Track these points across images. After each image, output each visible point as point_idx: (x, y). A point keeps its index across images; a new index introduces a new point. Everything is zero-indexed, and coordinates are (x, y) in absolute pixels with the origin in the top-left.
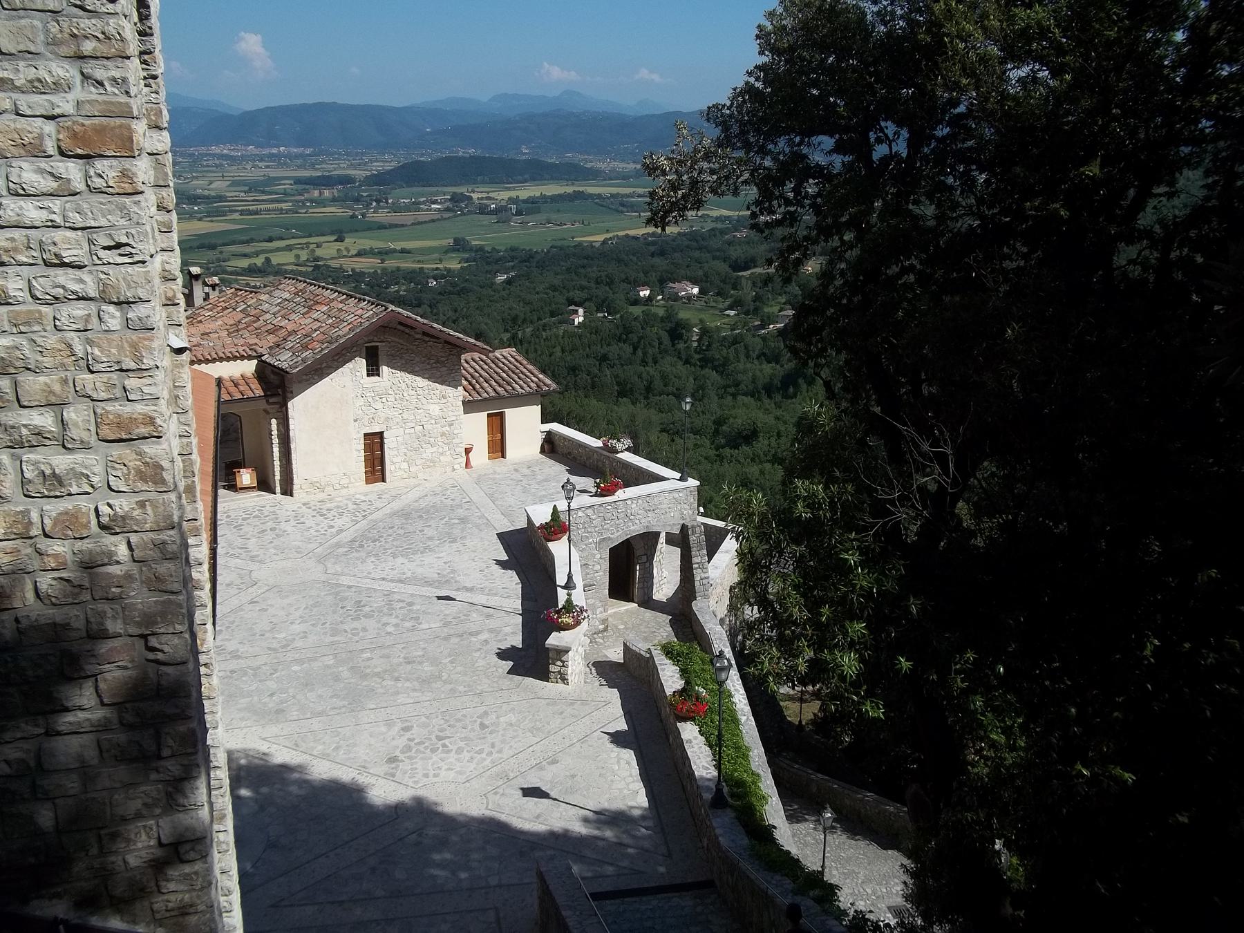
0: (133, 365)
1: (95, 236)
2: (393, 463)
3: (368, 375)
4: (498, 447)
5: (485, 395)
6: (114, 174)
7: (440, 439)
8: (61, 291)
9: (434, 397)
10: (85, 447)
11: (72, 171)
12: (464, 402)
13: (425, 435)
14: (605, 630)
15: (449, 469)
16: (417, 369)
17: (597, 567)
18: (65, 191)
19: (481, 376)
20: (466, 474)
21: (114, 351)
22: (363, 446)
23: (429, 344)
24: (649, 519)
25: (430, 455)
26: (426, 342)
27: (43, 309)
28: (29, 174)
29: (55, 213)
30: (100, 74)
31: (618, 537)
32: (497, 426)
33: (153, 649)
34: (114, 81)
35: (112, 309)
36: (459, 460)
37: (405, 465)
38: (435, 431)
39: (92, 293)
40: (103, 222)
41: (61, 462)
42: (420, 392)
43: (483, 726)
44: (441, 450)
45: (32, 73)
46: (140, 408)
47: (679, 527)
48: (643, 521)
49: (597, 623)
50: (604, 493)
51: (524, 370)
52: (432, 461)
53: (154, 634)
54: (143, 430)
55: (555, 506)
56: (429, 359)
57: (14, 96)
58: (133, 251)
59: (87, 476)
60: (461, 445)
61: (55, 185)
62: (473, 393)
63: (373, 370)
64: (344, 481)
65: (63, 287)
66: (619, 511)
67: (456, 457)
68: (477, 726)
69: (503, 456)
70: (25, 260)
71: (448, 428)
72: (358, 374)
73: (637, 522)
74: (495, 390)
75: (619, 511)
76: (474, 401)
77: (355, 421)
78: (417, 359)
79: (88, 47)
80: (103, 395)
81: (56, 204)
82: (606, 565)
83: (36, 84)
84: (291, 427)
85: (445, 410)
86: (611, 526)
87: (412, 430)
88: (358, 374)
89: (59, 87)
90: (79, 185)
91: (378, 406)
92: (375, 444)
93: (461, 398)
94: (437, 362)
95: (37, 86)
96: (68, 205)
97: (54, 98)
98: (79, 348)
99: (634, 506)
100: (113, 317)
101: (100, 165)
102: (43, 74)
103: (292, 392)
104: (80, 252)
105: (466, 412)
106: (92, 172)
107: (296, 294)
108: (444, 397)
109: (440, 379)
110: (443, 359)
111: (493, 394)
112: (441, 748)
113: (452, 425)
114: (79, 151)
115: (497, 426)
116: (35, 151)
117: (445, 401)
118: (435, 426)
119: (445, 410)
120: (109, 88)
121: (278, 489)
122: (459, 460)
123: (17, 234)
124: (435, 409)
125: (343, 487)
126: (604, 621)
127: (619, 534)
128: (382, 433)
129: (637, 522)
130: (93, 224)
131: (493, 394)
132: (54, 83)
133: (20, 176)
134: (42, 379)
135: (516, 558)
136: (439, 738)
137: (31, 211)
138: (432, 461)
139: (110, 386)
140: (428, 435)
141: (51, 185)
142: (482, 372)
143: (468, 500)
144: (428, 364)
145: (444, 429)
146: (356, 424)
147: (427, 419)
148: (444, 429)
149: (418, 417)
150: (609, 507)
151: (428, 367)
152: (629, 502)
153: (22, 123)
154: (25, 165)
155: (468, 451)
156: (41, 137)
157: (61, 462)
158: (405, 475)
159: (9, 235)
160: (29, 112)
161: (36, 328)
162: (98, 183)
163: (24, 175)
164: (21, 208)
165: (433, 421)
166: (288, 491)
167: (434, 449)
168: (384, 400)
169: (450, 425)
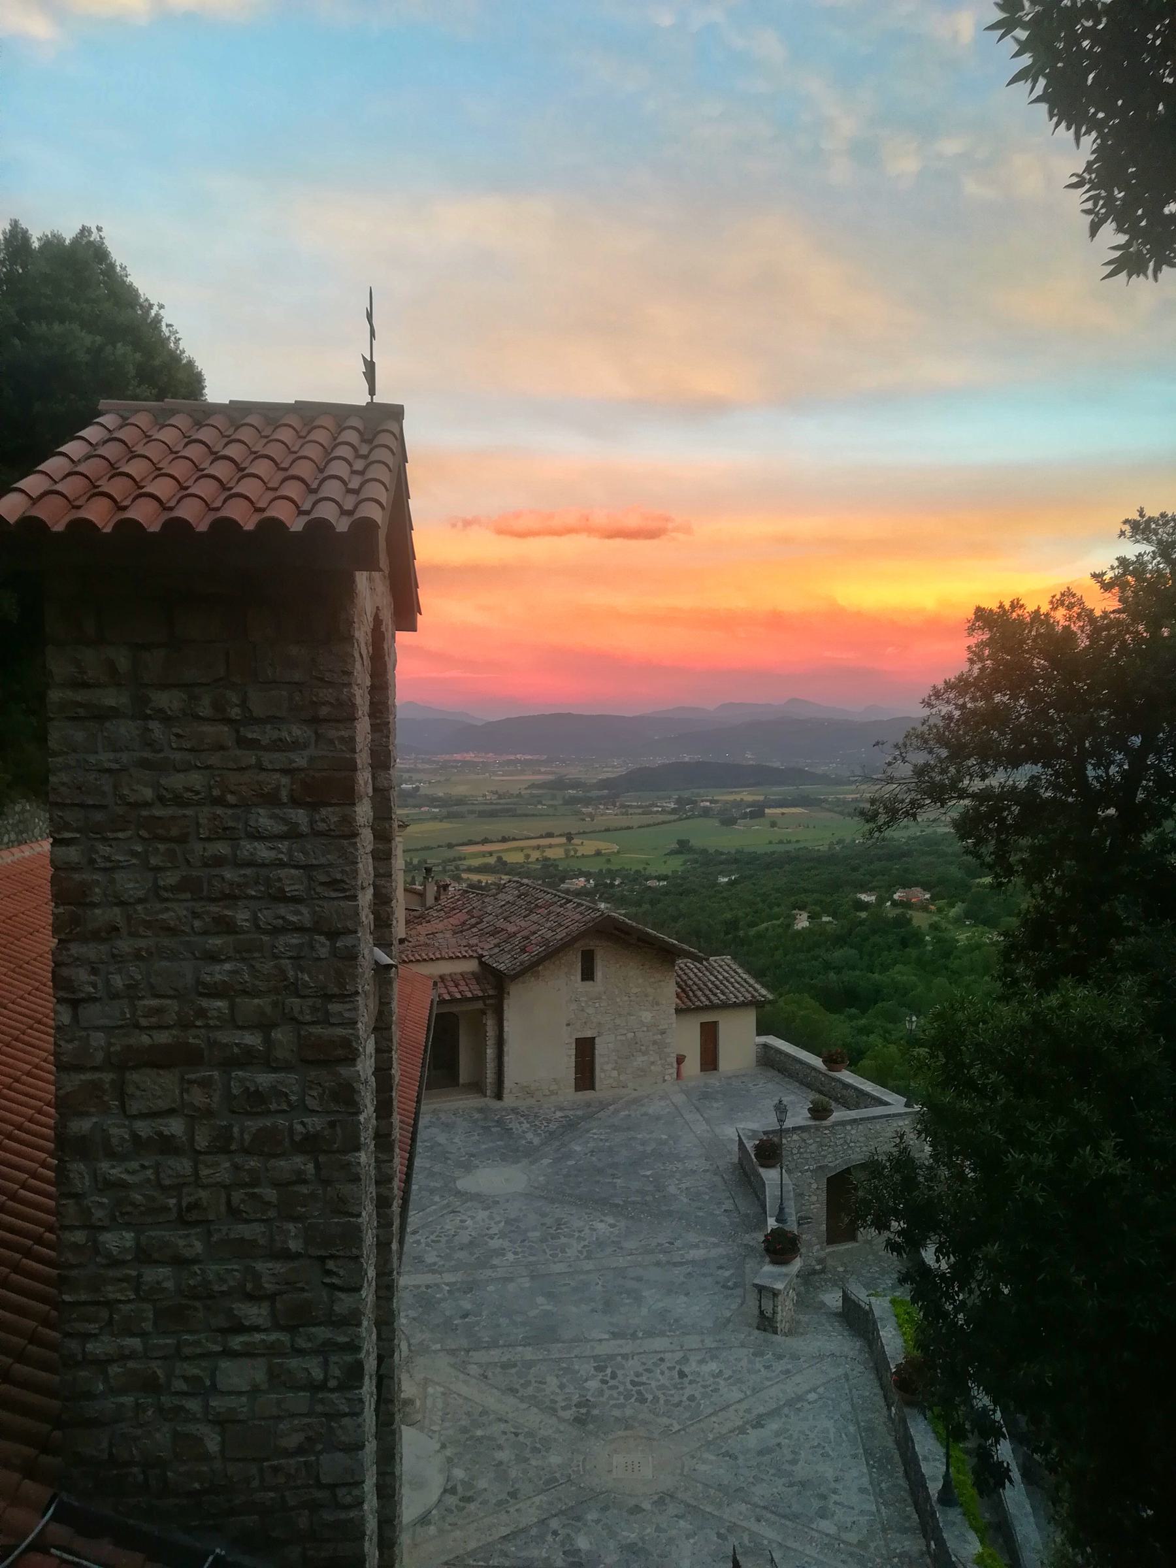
0: (336, 991)
1: (315, 873)
2: (603, 1070)
3: (583, 980)
4: (710, 1060)
5: (698, 1003)
6: (336, 819)
7: (651, 1048)
8: (281, 921)
10: (287, 1068)
11: (300, 816)
14: (823, 1271)
17: (814, 1198)
18: (293, 834)
19: (695, 983)
21: (321, 977)
22: (573, 1052)
27: (265, 938)
28: (263, 819)
29: (282, 853)
30: (332, 734)
31: (835, 1163)
32: (710, 1034)
33: (329, 1273)
34: (342, 739)
35: (322, 939)
36: (671, 1071)
37: (615, 1074)
39: (308, 923)
40: (323, 861)
41: (264, 1079)
43: (682, 1375)
44: (652, 1059)
45: (275, 735)
46: (340, 1031)
49: (814, 1263)
51: (739, 979)
53: (332, 1257)
54: (340, 1052)
57: (260, 753)
58: (346, 887)
59: (286, 1095)
61: (285, 828)
63: (588, 974)
64: (554, 1087)
65: (283, 918)
68: (675, 1374)
70: (254, 893)
71: (659, 1037)
72: (572, 978)
74: (709, 999)
77: (568, 1025)
79: (324, 711)
80: (308, 1018)
81: (284, 846)
82: (824, 1196)
83: (278, 743)
84: (506, 1029)
86: (830, 1153)
87: (623, 1038)
88: (572, 978)
89: (296, 746)
90: (305, 829)
91: (590, 1011)
92: (585, 1050)
93: (674, 1006)
95: (278, 745)
96: (294, 845)
97: (292, 755)
98: (291, 973)
99: (853, 1132)
100: (323, 945)
101: (324, 812)
102: (285, 734)
103: (509, 993)
104: (301, 888)
106: (317, 817)
107: (519, 897)
108: (658, 1004)
111: (707, 1003)
112: (636, 1396)
113: (664, 1033)
114: (308, 800)
115: (710, 1034)
116: (271, 799)
120: (339, 746)
121: (488, 1093)
122: (671, 1071)
123: (248, 871)
124: (647, 1016)
125: (552, 1093)
126: (821, 1261)
127: (837, 1162)
128: (594, 1038)
129: (858, 1149)
130: (315, 862)
131: (707, 1003)
132: (293, 742)
133: (257, 821)
134: (256, 1001)
136: (633, 1383)
137: (263, 852)
139: (314, 1009)
141: (283, 828)
142: (696, 980)
145: (655, 1037)
146: (569, 1028)
148: (655, 1037)
153: (263, 776)
154: (261, 811)
155: (680, 1060)
156: (278, 788)
157: (264, 1079)
158: (614, 1084)
159: (243, 872)
160: (270, 767)
161: (256, 955)
162: (322, 826)
163: (261, 820)
164: (255, 849)
165: (645, 1029)
166: (499, 1096)
167: (645, 1058)
168: (597, 1005)
169: (663, 1033)
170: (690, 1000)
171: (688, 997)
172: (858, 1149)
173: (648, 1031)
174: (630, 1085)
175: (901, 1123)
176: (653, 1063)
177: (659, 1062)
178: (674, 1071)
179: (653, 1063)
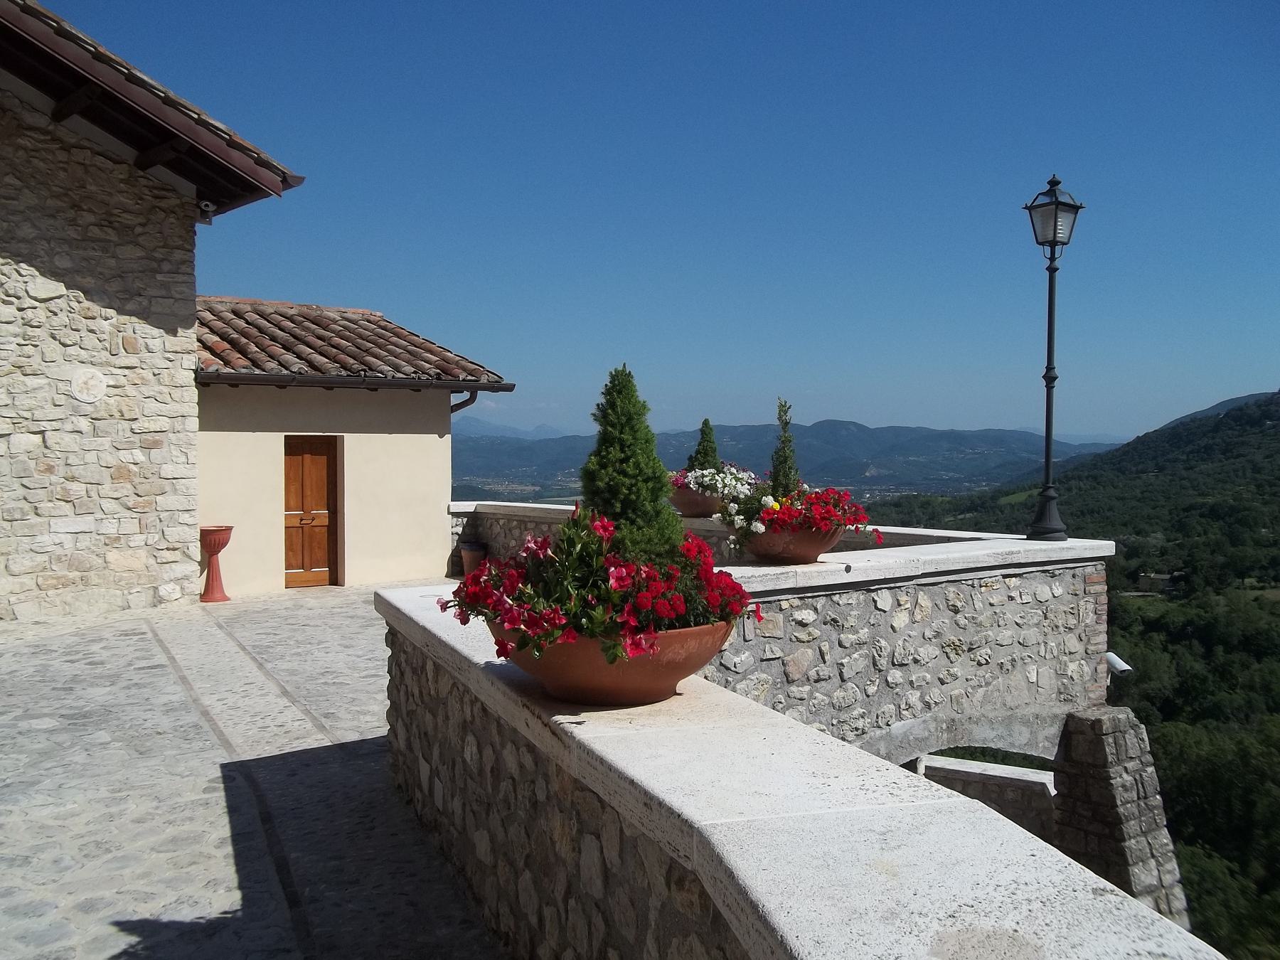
7: (106, 489)
9: (90, 341)
12: (203, 380)
13: (50, 469)
15: (140, 599)
16: (27, 231)
20: (200, 611)
23: (79, 155)
24: (956, 689)
25: (68, 541)
26: (67, 148)
38: (91, 457)
42: (40, 315)
44: (110, 528)
47: (1054, 730)
48: (935, 694)
50: (782, 542)
52: (72, 564)
55: (620, 386)
56: (76, 206)
60: (185, 518)
62: (235, 356)
66: (849, 638)
67: (168, 556)
69: (335, 579)
71: (139, 456)
73: (914, 697)
75: (849, 638)
76: (234, 382)
78: (29, 199)
85: (130, 390)
93: (190, 361)
94: (107, 221)
105: (209, 421)
108: (129, 347)
109: (114, 286)
110: (128, 219)
113: (156, 445)
117: (132, 360)
118: (88, 442)
119: (130, 390)
135: (294, 901)
138: (72, 564)
140: (62, 471)
143: (161, 659)
144: (73, 222)
147: (58, 413)
148: (125, 456)
149: (24, 401)
150: (807, 615)
151: (72, 233)
152: (884, 599)
155: (213, 541)
165: (84, 424)
167: (86, 523)
170: (255, 364)
171: (243, 352)
172: (914, 697)
173: (95, 432)
174: (27, 611)
175: (1044, 592)
176: (113, 541)
177: (138, 540)
178: (192, 568)
179: (113, 541)
